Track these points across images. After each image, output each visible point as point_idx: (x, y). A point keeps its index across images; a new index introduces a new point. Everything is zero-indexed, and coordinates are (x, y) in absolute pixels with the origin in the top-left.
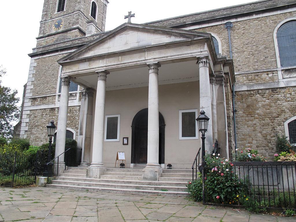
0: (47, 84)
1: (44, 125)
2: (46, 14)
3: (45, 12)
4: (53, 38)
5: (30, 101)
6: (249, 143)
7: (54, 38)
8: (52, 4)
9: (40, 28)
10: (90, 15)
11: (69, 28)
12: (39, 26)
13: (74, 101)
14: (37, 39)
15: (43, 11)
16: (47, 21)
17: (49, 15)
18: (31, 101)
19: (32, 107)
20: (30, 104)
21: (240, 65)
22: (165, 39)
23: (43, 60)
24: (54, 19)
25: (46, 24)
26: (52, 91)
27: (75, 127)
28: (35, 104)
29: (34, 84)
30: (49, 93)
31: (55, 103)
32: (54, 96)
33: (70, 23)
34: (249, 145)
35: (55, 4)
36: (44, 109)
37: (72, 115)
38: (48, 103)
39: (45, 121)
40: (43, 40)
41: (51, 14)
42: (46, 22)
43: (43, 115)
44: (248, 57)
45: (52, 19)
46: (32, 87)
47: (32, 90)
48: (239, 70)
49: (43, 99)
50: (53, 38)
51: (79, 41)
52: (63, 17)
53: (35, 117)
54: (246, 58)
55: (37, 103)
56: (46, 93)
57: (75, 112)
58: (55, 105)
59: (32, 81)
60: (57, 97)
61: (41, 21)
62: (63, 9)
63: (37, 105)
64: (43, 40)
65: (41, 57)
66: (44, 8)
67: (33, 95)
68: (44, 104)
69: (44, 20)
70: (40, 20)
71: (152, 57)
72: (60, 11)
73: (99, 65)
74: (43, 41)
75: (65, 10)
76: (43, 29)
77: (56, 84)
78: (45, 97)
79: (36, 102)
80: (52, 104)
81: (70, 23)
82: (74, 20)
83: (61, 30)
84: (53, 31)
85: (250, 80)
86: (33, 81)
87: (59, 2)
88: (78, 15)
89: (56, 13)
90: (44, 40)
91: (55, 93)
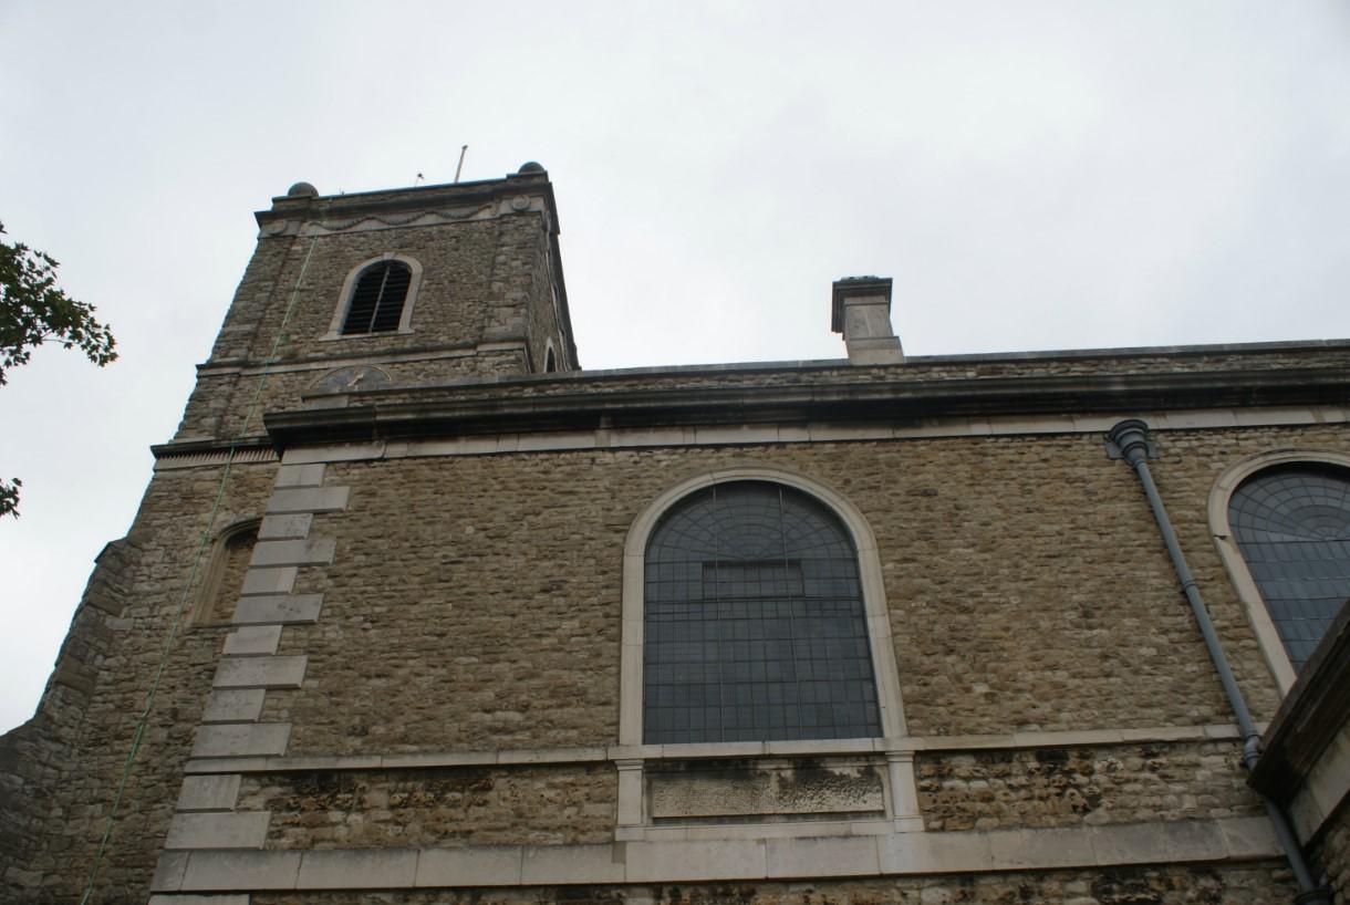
2: (254, 336)
3: (248, 321)
5: (259, 801)
8: (302, 291)
9: (196, 399)
12: (189, 383)
14: (159, 452)
15: (231, 317)
16: (257, 365)
18: (273, 805)
20: (253, 827)
23: (427, 472)
24: (313, 366)
25: (243, 383)
26: (552, 724)
28: (326, 832)
29: (314, 651)
30: (524, 736)
31: (619, 835)
32: (590, 766)
35: (332, 295)
38: (512, 836)
40: (207, 468)
42: (247, 372)
46: (294, 671)
47: (287, 701)
49: (446, 789)
55: (346, 823)
59: (286, 625)
60: (631, 785)
61: (210, 365)
62: (389, 321)
64: (207, 468)
65: (398, 450)
66: (242, 304)
67: (297, 746)
68: (448, 843)
70: (204, 356)
72: (366, 332)
74: (215, 473)
76: (218, 404)
78: (474, 778)
79: (335, 816)
80: (574, 844)
86: (310, 623)
87: (357, 291)
88: (512, 362)
89: (334, 335)
90: (216, 467)
91: (612, 735)
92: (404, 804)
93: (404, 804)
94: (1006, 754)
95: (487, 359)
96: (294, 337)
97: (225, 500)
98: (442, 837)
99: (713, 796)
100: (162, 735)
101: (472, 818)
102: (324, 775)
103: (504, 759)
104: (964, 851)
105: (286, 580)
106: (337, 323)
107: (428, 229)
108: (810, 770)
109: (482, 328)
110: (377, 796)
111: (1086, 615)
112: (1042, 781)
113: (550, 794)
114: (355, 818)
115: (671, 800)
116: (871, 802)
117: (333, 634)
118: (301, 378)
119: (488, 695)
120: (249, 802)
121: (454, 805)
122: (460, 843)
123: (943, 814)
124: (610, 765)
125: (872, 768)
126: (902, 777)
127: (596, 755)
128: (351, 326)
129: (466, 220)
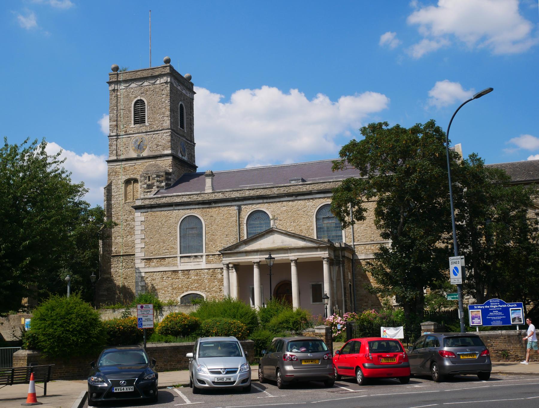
0: (164, 243)
1: (166, 289)
4: (134, 164)
6: (366, 303)
7: (137, 164)
10: (179, 127)
11: (157, 153)
13: (200, 263)
16: (120, 136)
17: (122, 127)
18: (145, 262)
19: (148, 268)
21: (359, 236)
22: (301, 243)
24: (131, 136)
25: (119, 140)
27: (204, 291)
30: (168, 253)
32: (175, 257)
33: (158, 145)
34: (366, 304)
35: (130, 111)
36: (164, 271)
37: (200, 278)
38: (167, 265)
39: (167, 284)
40: (117, 165)
41: (125, 126)
43: (164, 277)
44: (366, 229)
45: (127, 134)
48: (358, 241)
50: (134, 164)
51: (198, 196)
52: (145, 134)
53: (154, 280)
54: (366, 230)
56: (163, 253)
57: (202, 275)
58: (178, 267)
59: (141, 239)
60: (179, 258)
62: (142, 121)
63: (154, 267)
69: (114, 134)
71: (292, 256)
73: (256, 258)
75: (147, 124)
77: (175, 244)
78: (164, 258)
80: (174, 266)
81: (158, 145)
82: (164, 141)
83: (145, 154)
84: (134, 155)
85: (367, 250)
89: (133, 126)
90: (119, 165)
91: (176, 253)
92: (158, 262)
93: (158, 262)
94: (215, 255)
95: (164, 134)
96: (125, 126)
97: (123, 173)
98: (161, 265)
99: (186, 260)
100: (125, 224)
101: (164, 263)
102: (149, 259)
103: (167, 256)
104: (209, 266)
105: (139, 232)
106: (133, 122)
107: (146, 87)
108: (196, 256)
109: (162, 124)
110: (154, 261)
111: (227, 236)
112: (218, 258)
113: (171, 260)
114: (153, 263)
115: (183, 260)
116: (201, 260)
117: (147, 240)
118: (129, 139)
119: (164, 248)
120: (142, 262)
121: (162, 262)
122: (163, 266)
123: (208, 262)
124: (177, 257)
125: (202, 256)
126: (204, 257)
127: (175, 256)
128: (136, 122)
129: (154, 84)
